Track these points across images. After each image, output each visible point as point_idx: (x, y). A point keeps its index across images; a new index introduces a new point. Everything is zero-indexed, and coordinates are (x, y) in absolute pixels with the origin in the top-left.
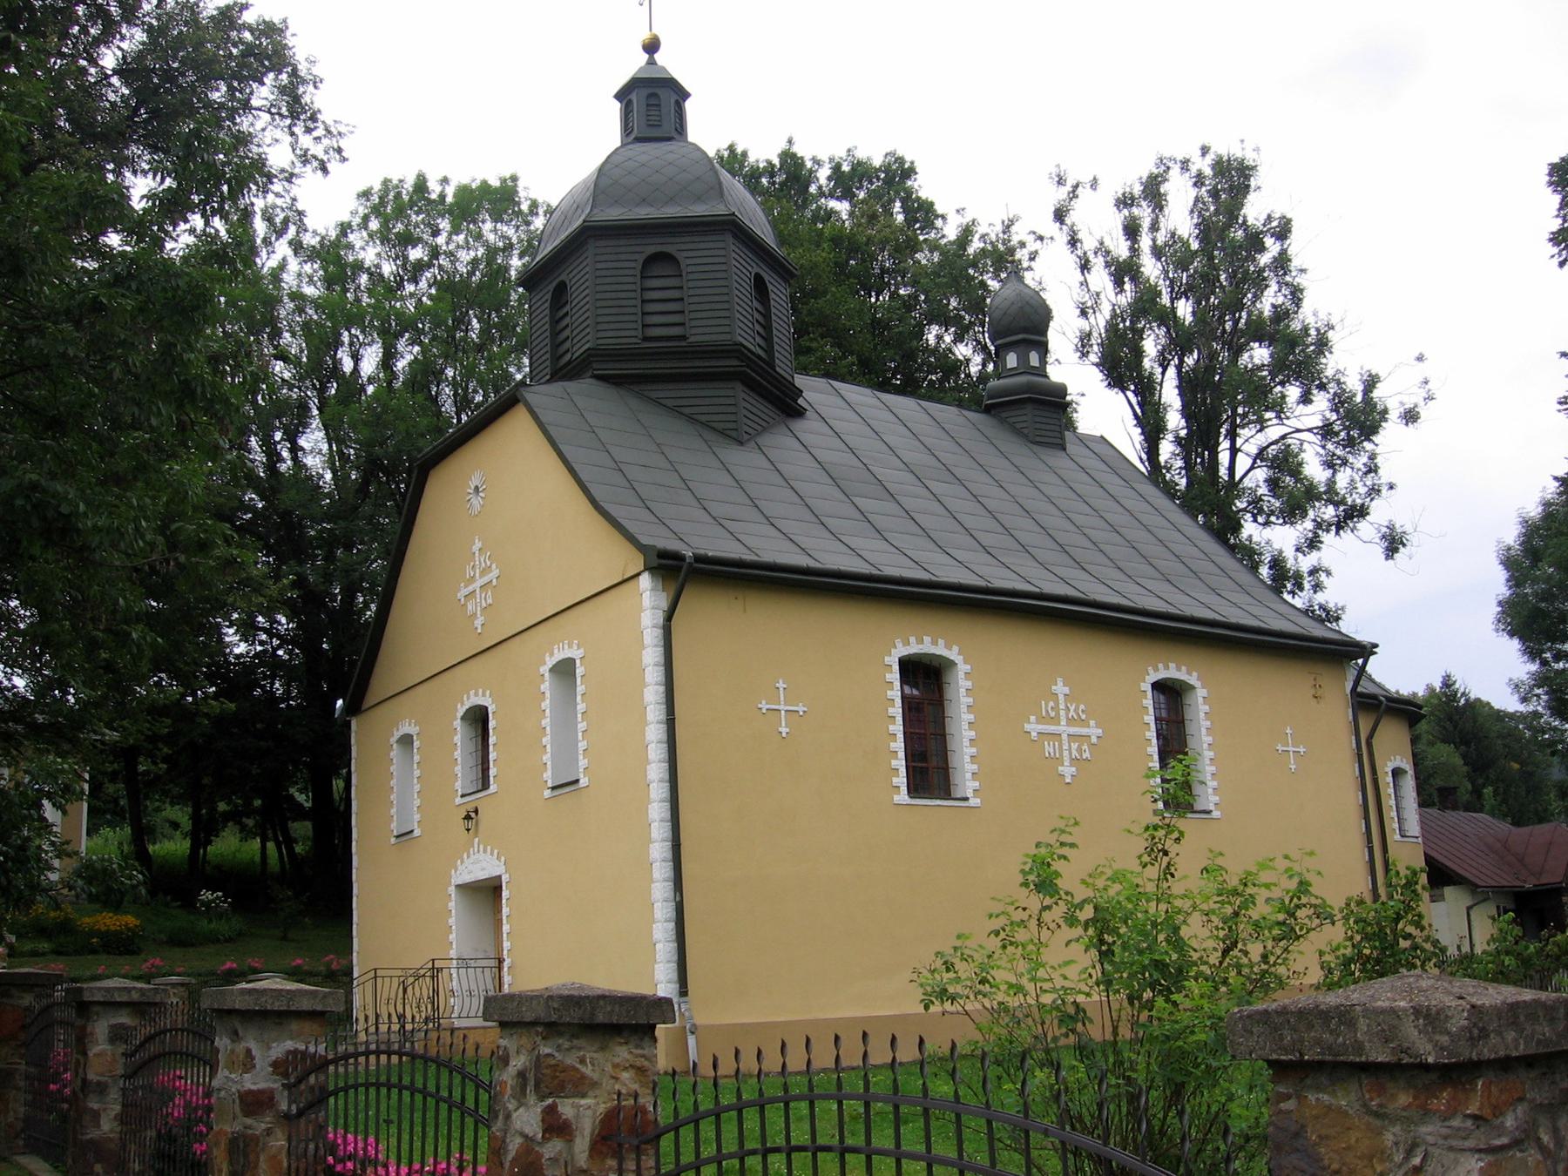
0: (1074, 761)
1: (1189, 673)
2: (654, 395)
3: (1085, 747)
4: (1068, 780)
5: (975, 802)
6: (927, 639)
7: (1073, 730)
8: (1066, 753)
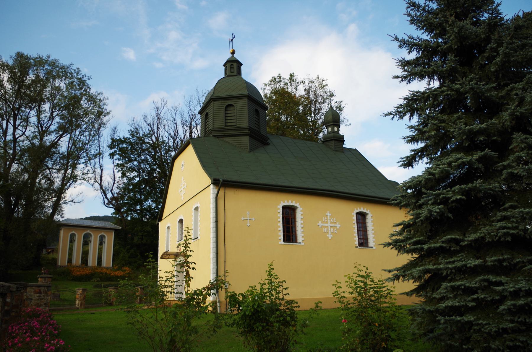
0: (332, 233)
1: (367, 210)
2: (227, 140)
3: (335, 229)
4: (330, 238)
5: (302, 244)
6: (290, 201)
8: (329, 231)
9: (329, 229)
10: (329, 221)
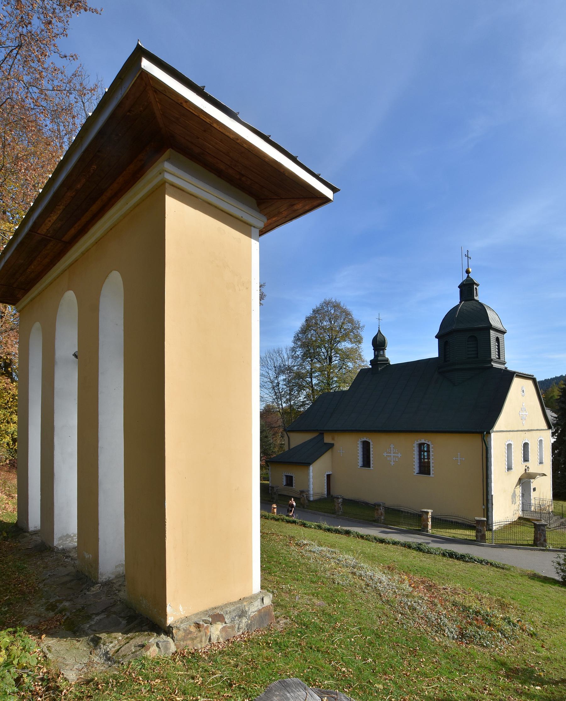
0: (394, 461)
10: (392, 452)
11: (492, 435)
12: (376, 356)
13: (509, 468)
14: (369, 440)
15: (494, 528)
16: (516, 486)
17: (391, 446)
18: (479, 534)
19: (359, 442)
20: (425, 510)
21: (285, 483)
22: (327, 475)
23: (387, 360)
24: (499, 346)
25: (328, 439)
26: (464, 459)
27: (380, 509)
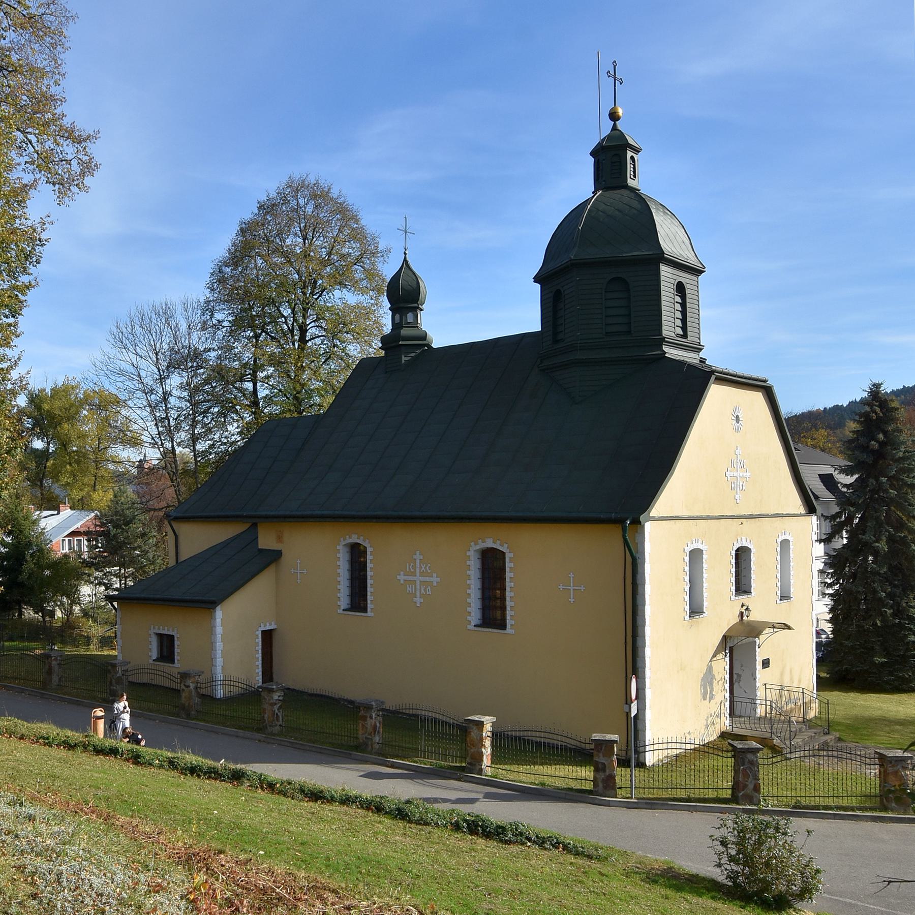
0: (422, 596)
7: (422, 579)
9: (418, 587)
10: (418, 571)
11: (648, 526)
12: (396, 326)
13: (695, 610)
14: (364, 541)
15: (651, 759)
16: (714, 656)
17: (415, 557)
18: (601, 775)
19: (340, 547)
20: (476, 718)
21: (154, 654)
22: (264, 633)
23: (424, 337)
24: (683, 305)
25: (266, 540)
26: (582, 588)
27: (371, 718)
